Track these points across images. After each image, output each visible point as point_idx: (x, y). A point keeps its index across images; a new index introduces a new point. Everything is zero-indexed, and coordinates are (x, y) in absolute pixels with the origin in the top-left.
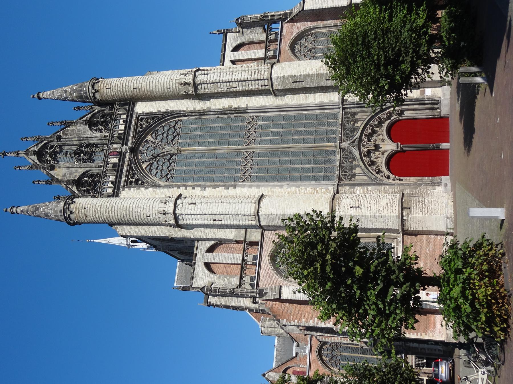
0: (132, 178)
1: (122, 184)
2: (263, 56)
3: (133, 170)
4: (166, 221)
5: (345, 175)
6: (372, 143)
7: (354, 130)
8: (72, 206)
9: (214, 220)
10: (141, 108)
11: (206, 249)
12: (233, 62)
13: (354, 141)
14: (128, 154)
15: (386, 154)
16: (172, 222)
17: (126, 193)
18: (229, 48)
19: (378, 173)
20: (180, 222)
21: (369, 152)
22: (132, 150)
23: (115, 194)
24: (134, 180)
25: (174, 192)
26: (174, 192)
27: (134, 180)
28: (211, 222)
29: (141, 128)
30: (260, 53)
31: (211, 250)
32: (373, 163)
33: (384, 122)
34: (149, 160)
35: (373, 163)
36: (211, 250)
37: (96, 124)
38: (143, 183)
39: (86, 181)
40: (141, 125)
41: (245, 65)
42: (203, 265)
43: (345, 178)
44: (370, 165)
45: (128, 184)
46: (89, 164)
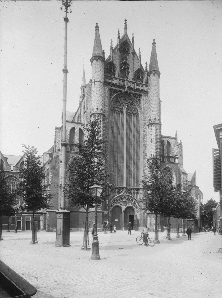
0: (113, 92)
3: (117, 93)
5: (113, 189)
12: (163, 141)
16: (93, 112)
24: (112, 93)
27: (112, 93)
31: (80, 130)
33: (134, 205)
36: (80, 130)
37: (139, 73)
39: (112, 68)
40: (137, 97)
43: (111, 189)
44: (116, 199)
45: (111, 90)
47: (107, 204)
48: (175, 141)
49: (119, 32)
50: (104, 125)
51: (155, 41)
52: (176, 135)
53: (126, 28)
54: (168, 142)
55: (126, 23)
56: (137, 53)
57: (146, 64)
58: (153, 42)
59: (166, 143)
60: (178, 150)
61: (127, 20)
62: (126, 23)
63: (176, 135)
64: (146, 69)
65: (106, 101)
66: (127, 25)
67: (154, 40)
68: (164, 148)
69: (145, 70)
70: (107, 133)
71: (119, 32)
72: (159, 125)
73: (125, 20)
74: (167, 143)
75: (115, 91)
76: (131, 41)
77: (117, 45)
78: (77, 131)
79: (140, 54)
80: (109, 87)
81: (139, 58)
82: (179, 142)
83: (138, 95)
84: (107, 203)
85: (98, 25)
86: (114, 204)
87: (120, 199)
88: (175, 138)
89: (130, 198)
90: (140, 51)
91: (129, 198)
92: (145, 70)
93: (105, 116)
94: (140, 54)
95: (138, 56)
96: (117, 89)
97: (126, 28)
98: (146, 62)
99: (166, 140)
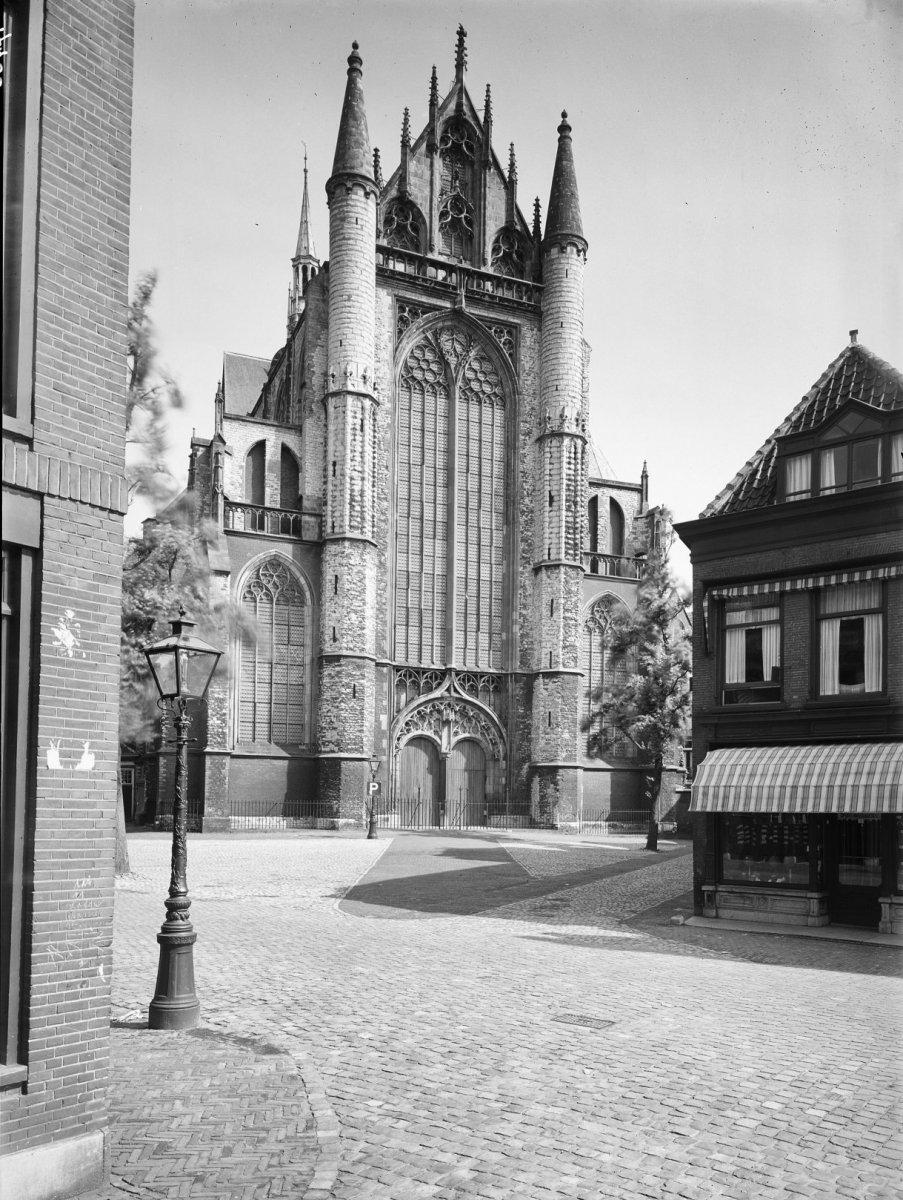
0: (410, 311)
1: (402, 293)
2: (599, 552)
3: (424, 313)
4: (333, 376)
6: (452, 717)
7: (473, 690)
8: (361, 193)
9: (334, 464)
10: (528, 336)
11: (288, 444)
12: (594, 501)
13: (456, 690)
14: (448, 305)
15: (436, 738)
16: (333, 388)
17: (386, 299)
18: (615, 493)
19: (407, 724)
20: (332, 402)
21: (440, 712)
22: (457, 313)
23: (384, 276)
24: (406, 314)
25: (384, 394)
26: (384, 394)
28: (331, 458)
29: (496, 331)
30: (605, 546)
32: (422, 717)
34: (438, 344)
35: (422, 717)
38: (400, 332)
40: (502, 332)
41: (586, 522)
42: (260, 438)
44: (419, 713)
45: (401, 303)
46: (436, 225)
47: (384, 732)
48: (635, 496)
49: (434, 79)
50: (375, 437)
51: (569, 121)
52: (645, 476)
53: (460, 65)
54: (615, 505)
55: (461, 45)
56: (504, 165)
57: (537, 206)
58: (559, 121)
59: (604, 509)
60: (647, 532)
61: (466, 29)
62: (461, 45)
63: (645, 476)
64: (537, 222)
65: (382, 345)
66: (465, 52)
67: (564, 115)
68: (599, 527)
69: (531, 229)
70: (387, 467)
71: (434, 79)
72: (579, 442)
73: (458, 33)
74: (608, 507)
75: (417, 309)
76: (481, 116)
77: (430, 130)
78: (272, 454)
79: (512, 165)
80: (402, 293)
81: (510, 186)
82: (652, 504)
83: (506, 325)
84: (384, 726)
85: (361, 53)
86: (408, 731)
87: (431, 712)
88: (641, 490)
89: (468, 707)
90: (512, 155)
91: (465, 708)
92: (531, 229)
93: (378, 404)
94: (512, 165)
95: (507, 174)
96: (424, 299)
97: (460, 65)
98: (537, 200)
99: (604, 496)
